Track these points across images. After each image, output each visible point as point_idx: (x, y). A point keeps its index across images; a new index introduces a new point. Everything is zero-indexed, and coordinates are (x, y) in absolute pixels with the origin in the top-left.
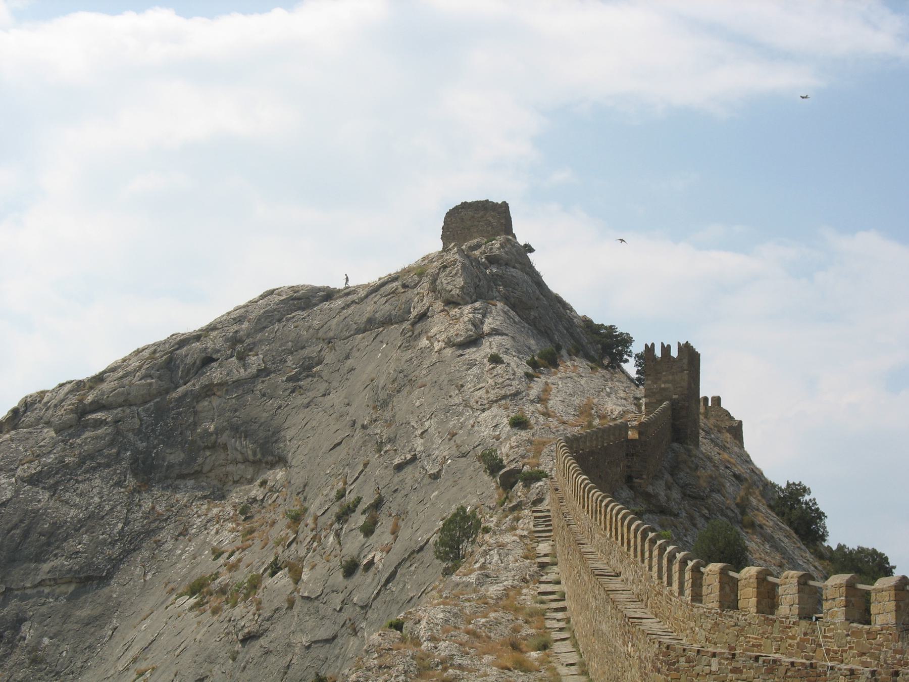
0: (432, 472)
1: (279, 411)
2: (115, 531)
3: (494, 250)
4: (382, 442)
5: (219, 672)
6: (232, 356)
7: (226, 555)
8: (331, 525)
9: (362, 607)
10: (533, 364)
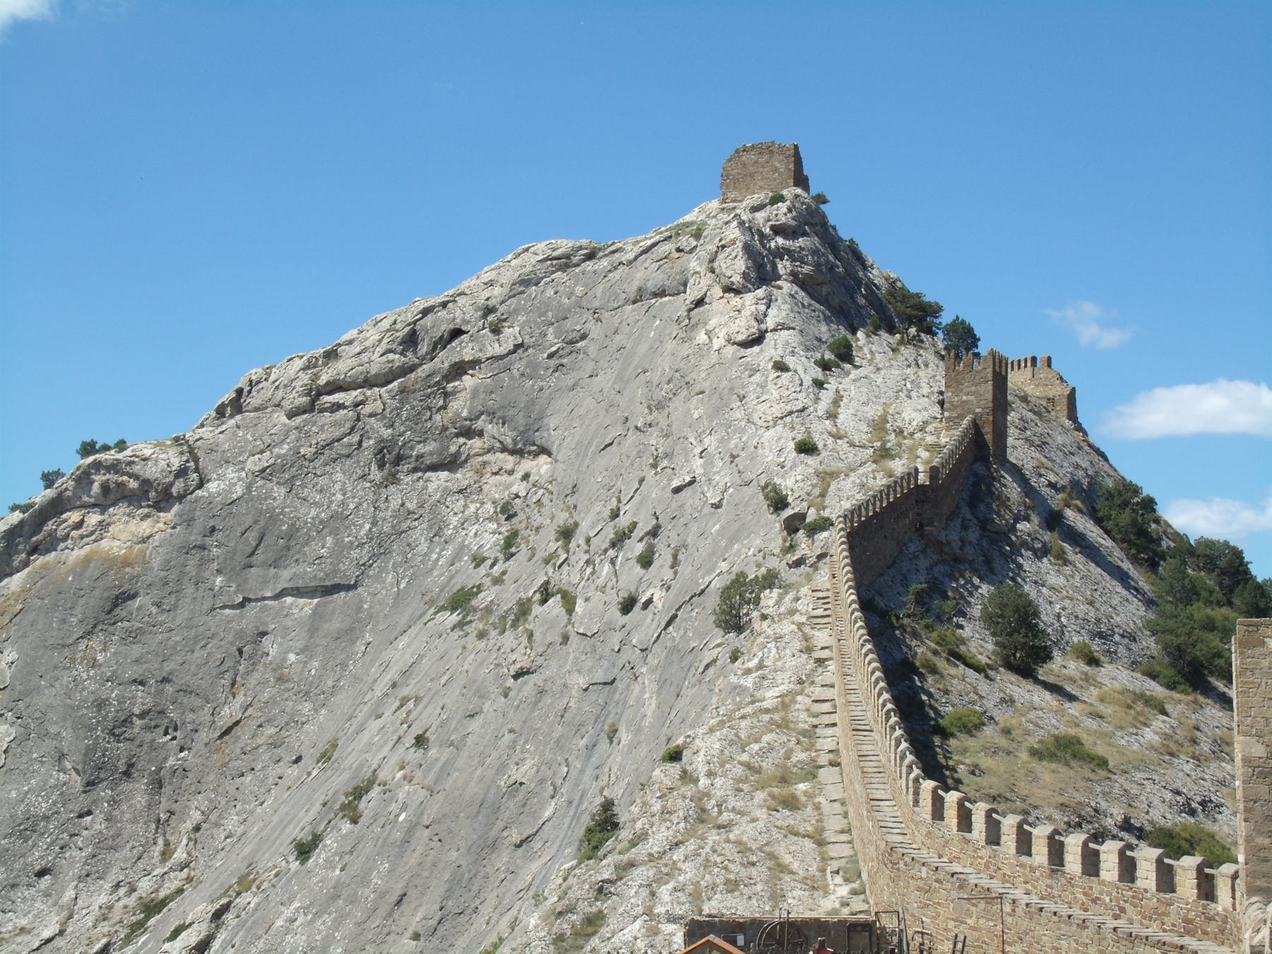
0: (713, 501)
1: (541, 394)
2: (362, 533)
3: (779, 217)
4: (657, 457)
5: (491, 710)
6: (484, 328)
7: (489, 562)
8: (606, 551)
9: (642, 650)
10: (825, 366)
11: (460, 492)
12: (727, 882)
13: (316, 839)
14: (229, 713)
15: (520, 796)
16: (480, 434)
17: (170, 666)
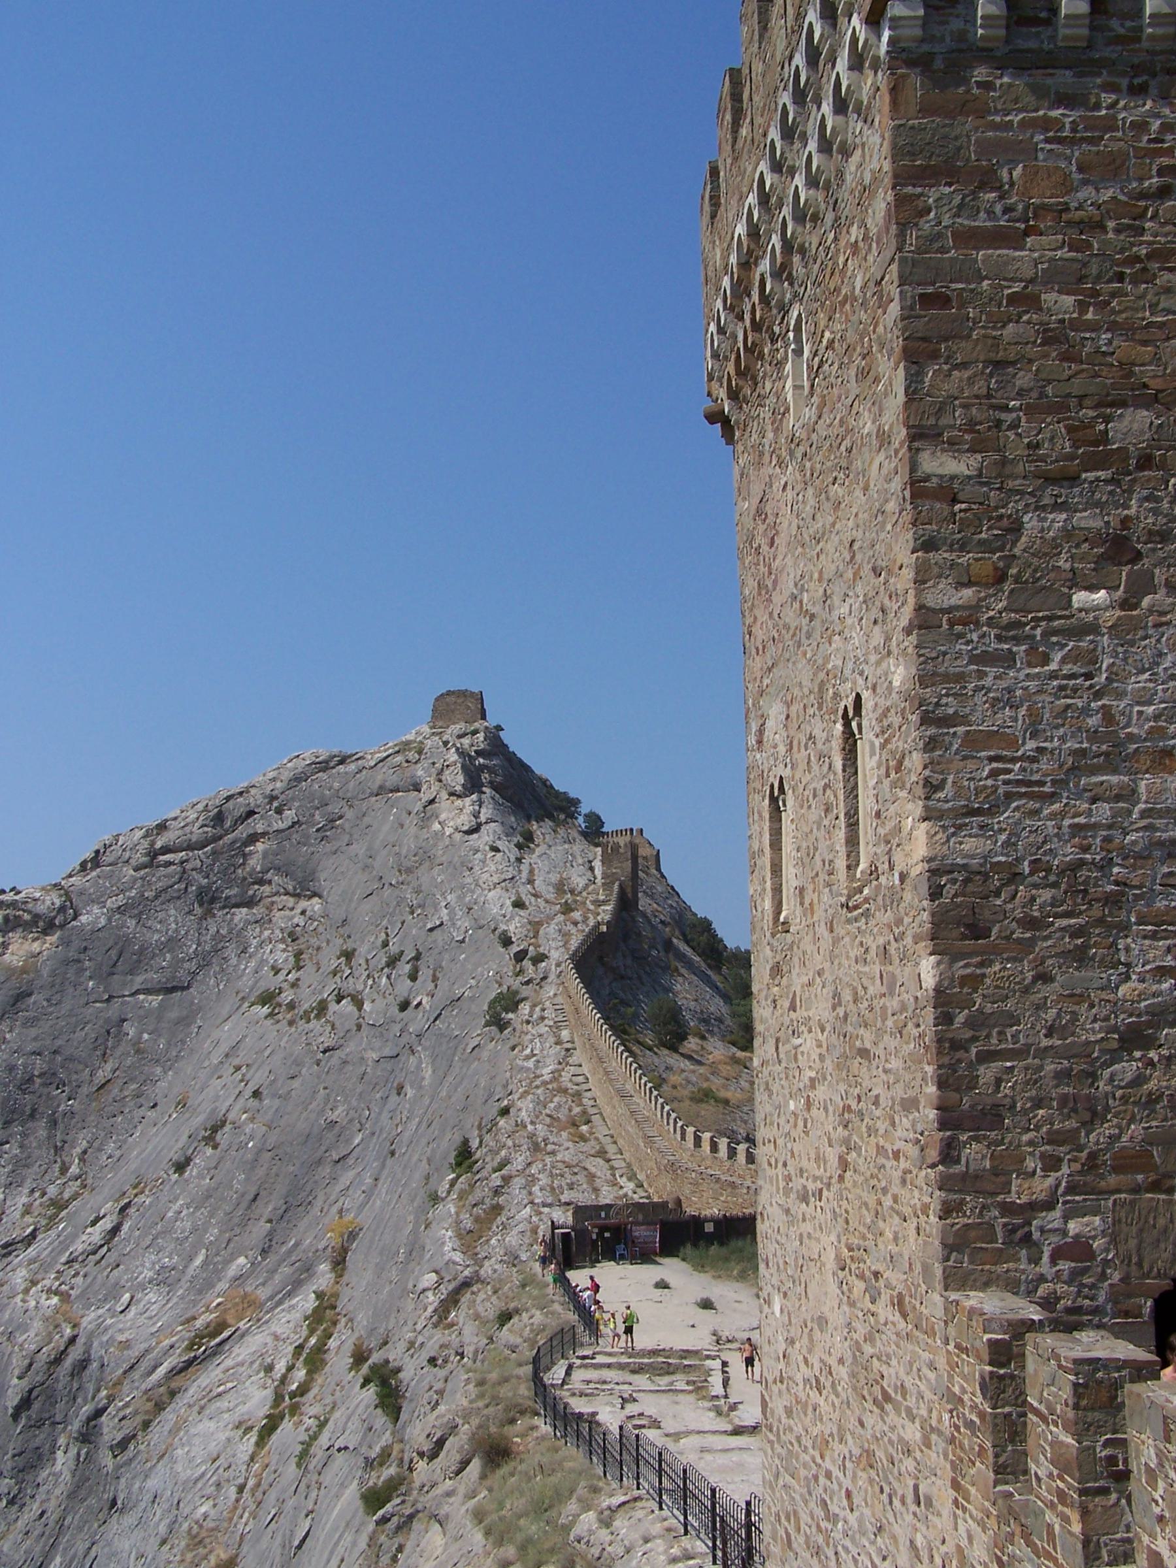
11: (256, 922)
12: (568, 1184)
13: (188, 1160)
14: (101, 1075)
15: (337, 1128)
16: (270, 882)
17: (59, 1042)
